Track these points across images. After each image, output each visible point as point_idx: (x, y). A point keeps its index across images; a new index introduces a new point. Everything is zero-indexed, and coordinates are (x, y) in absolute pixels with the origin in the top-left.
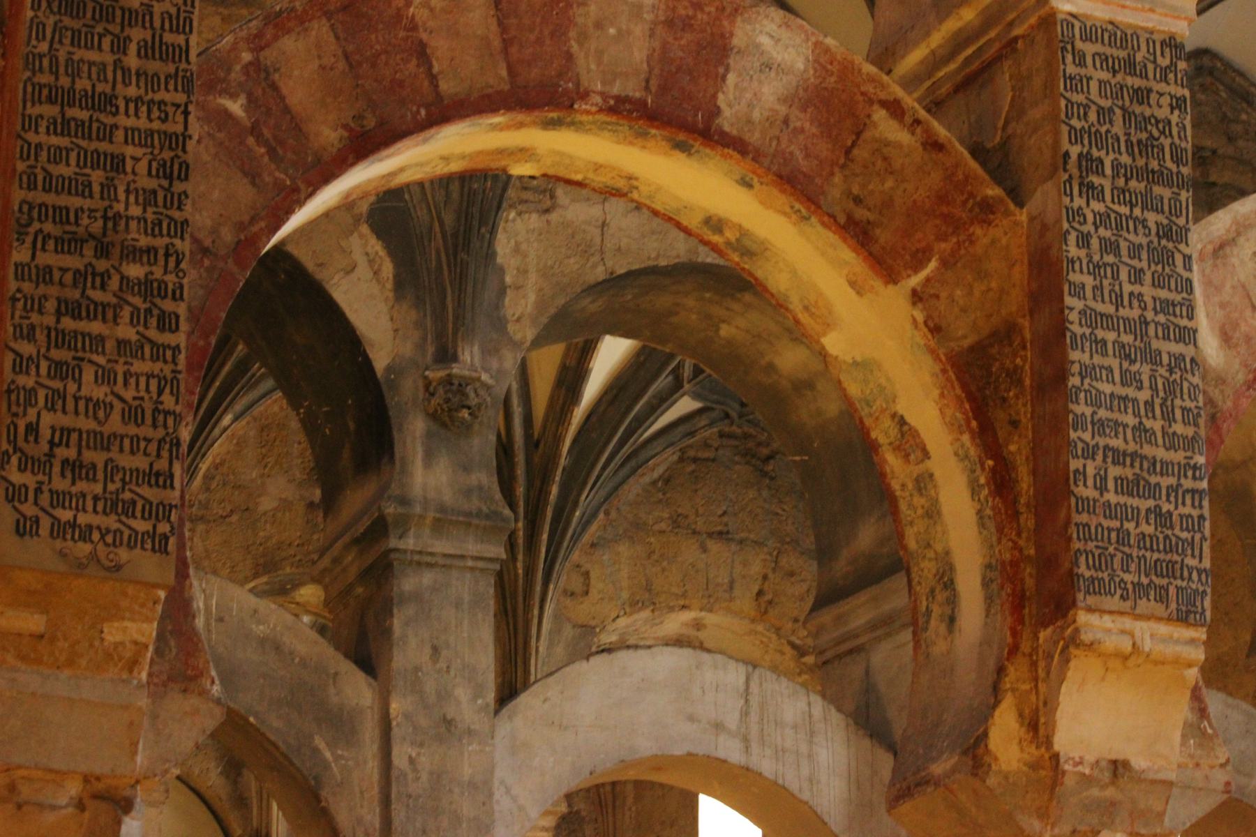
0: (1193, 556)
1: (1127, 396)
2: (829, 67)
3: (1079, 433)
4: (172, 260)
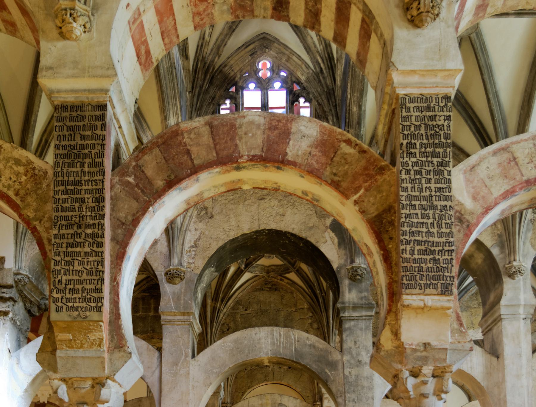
0: (448, 272)
3: (404, 237)
4: (100, 227)
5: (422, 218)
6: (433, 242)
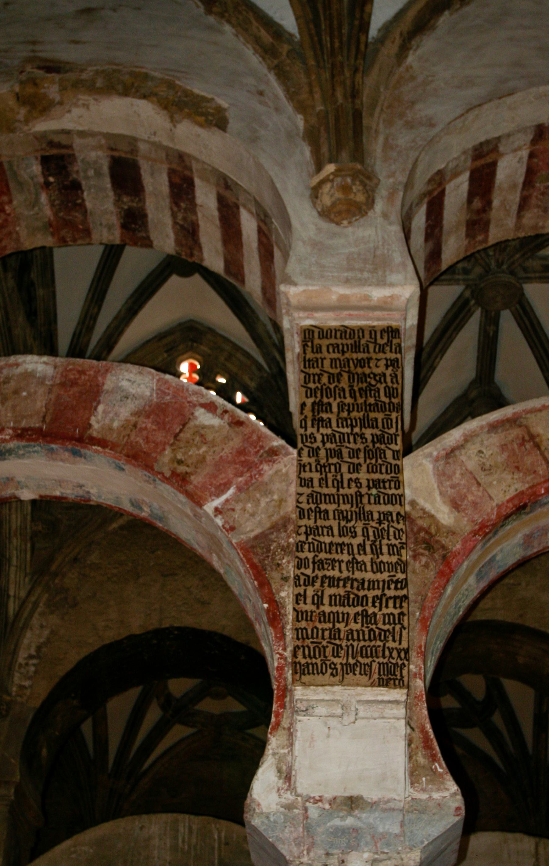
1: (343, 543)
2: (167, 391)
3: (303, 570)
5: (340, 536)
6: (363, 580)
